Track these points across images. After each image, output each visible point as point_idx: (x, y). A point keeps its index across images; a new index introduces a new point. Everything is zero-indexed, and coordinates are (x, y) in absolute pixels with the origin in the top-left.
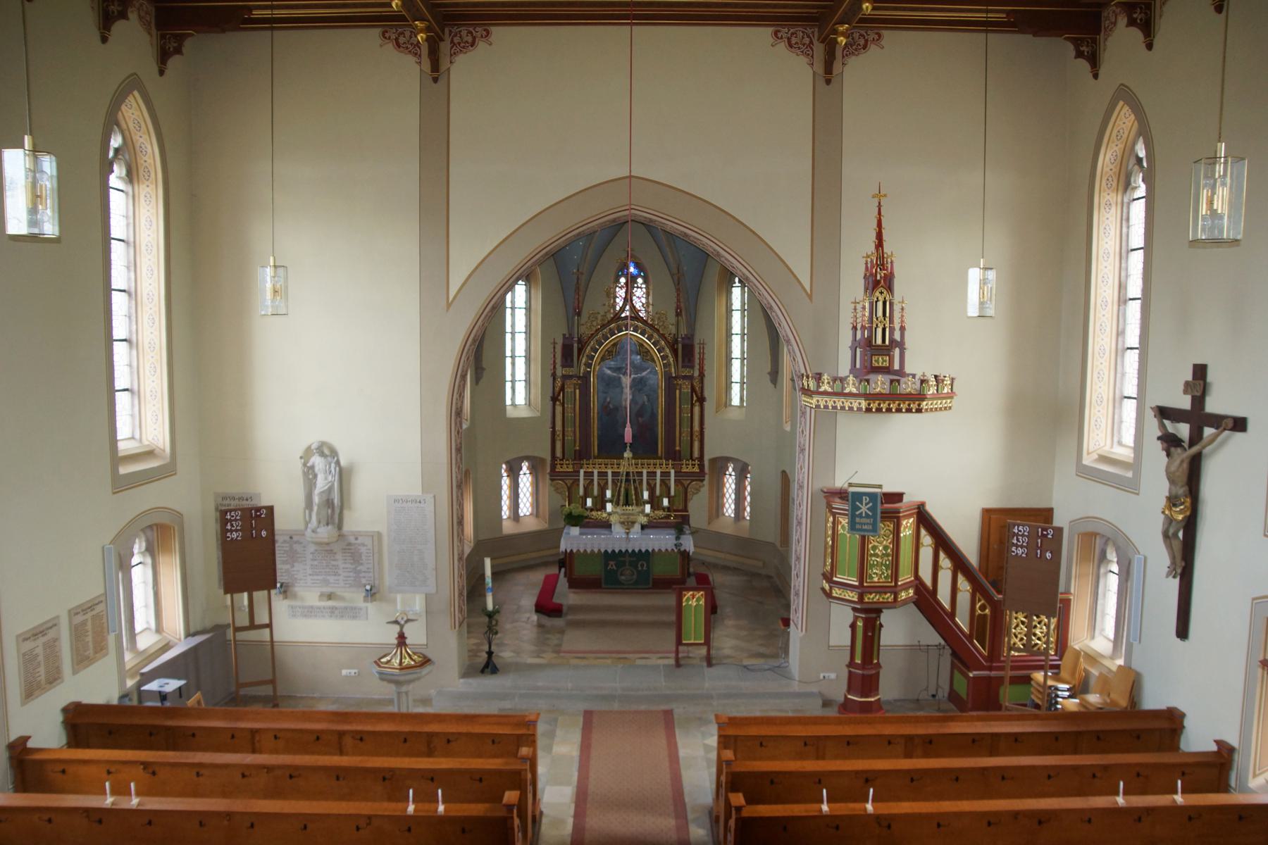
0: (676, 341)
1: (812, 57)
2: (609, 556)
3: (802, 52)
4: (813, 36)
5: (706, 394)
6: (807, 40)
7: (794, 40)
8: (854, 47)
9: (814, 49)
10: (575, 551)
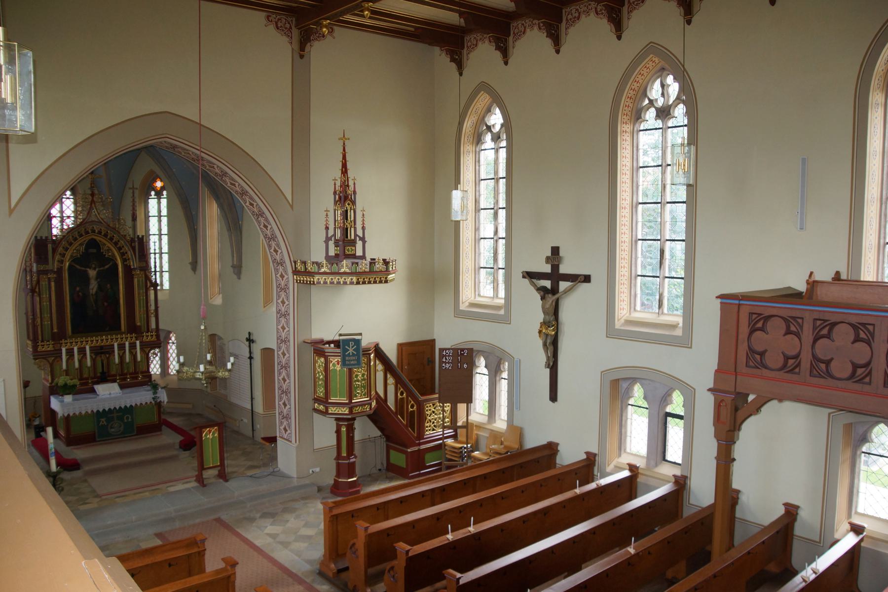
2: (100, 415)
10: (71, 415)
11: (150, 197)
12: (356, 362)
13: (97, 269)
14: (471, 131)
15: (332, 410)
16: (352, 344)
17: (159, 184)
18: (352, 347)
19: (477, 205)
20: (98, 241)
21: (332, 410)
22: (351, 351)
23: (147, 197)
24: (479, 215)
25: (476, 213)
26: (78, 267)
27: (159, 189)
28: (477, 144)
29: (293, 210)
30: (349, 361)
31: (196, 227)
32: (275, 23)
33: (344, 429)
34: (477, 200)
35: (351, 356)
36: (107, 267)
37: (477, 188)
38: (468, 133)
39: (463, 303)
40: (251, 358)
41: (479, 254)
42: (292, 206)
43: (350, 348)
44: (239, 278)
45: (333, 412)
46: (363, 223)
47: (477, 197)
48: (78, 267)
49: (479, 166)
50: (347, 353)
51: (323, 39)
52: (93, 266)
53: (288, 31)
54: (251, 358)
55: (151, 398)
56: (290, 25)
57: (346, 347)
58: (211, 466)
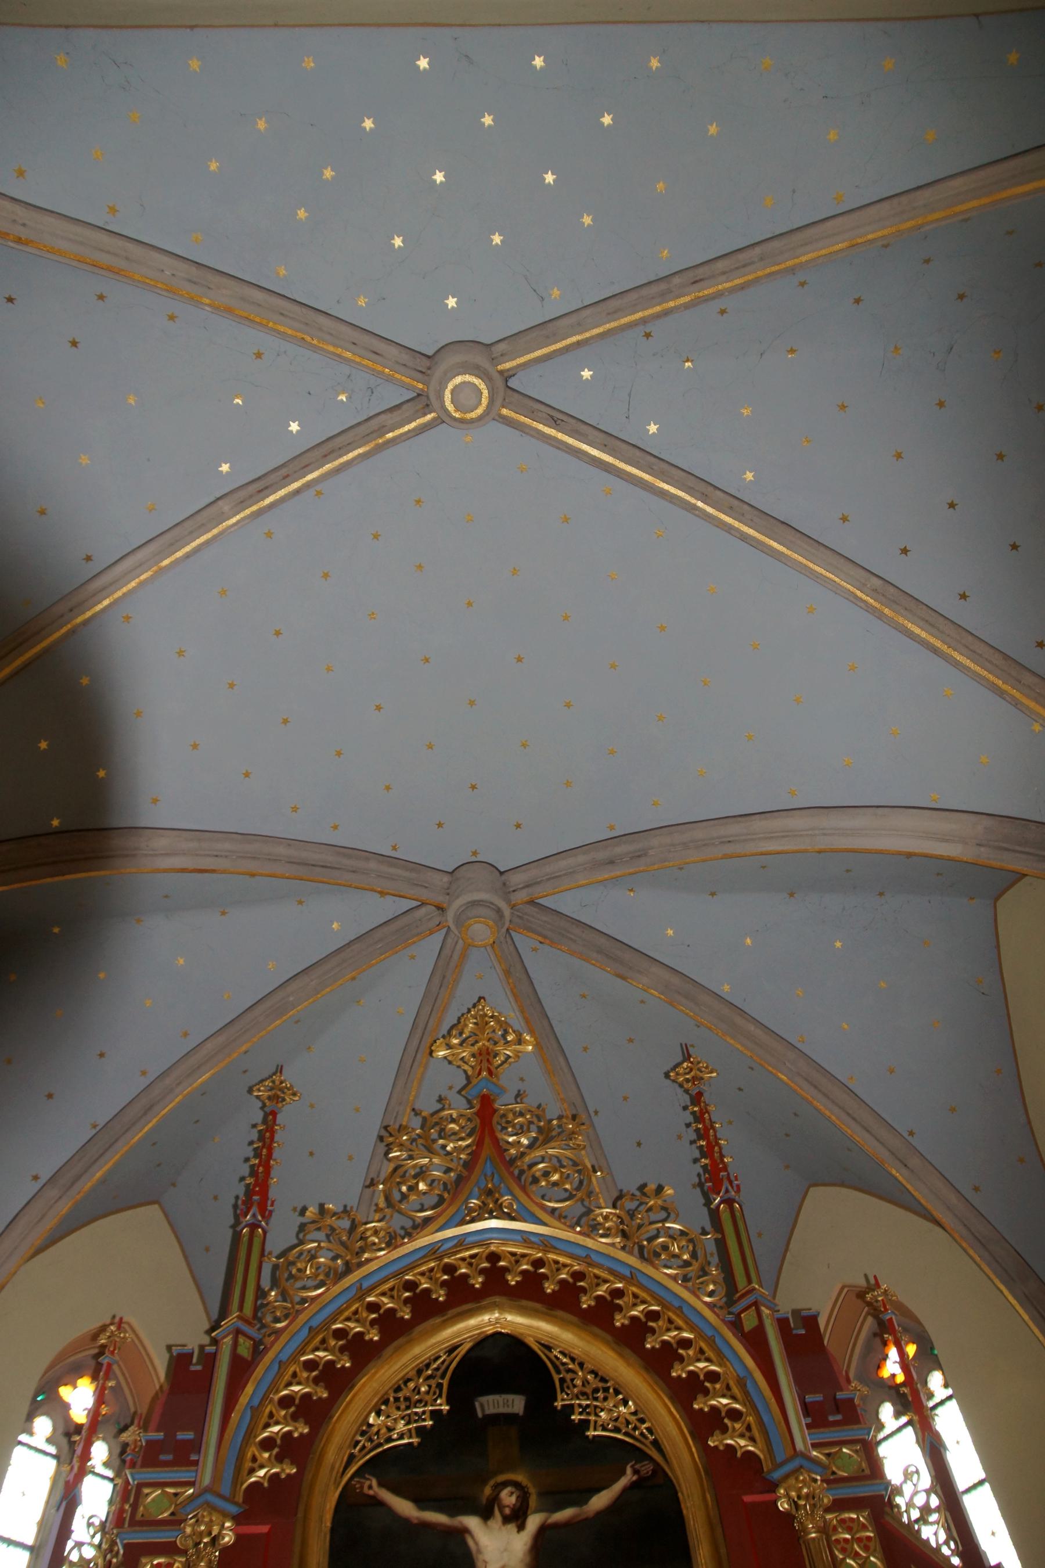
13: (534, 1522)
20: (535, 1347)
26: (404, 1507)
36: (600, 1501)
48: (404, 1507)
52: (509, 1498)
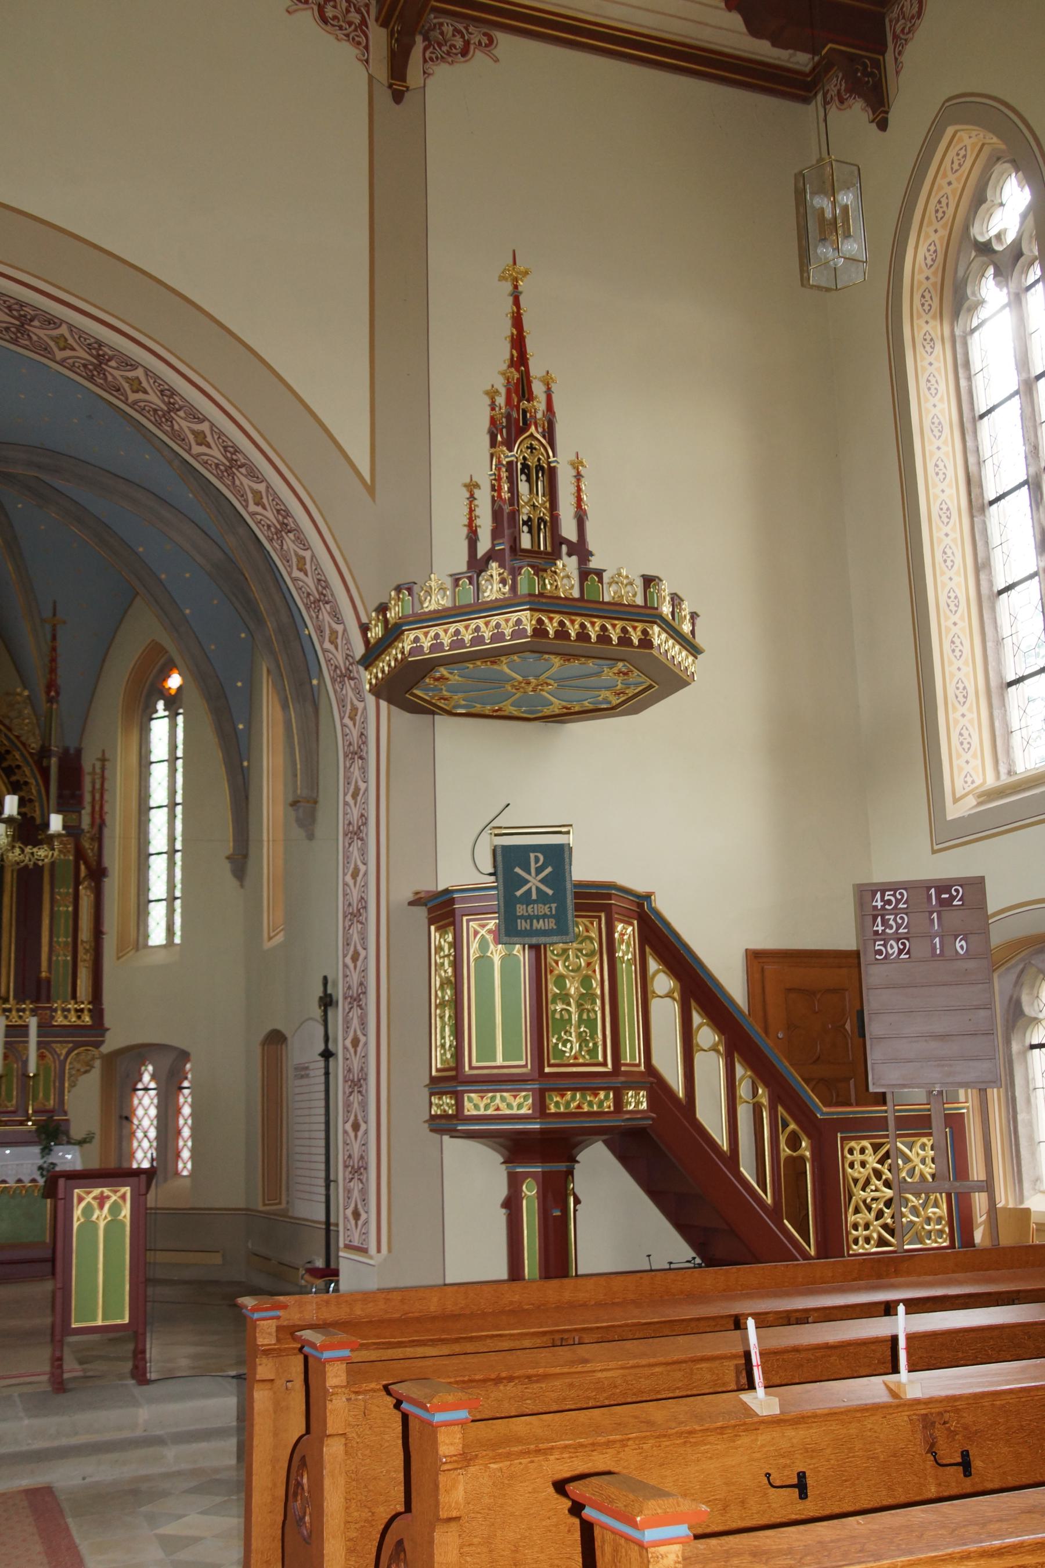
0: (44, 752)
1: (367, 48)
3: (347, 35)
4: (368, 13)
5: (107, 862)
6: (355, 18)
7: (330, 12)
8: (445, 49)
9: (370, 36)
11: (155, 716)
12: (551, 924)
14: (932, 279)
15: (477, 1107)
16: (537, 859)
17: (174, 681)
18: (539, 871)
19: (975, 491)
21: (475, 1104)
22: (534, 882)
23: (149, 714)
24: (984, 523)
25: (972, 517)
27: (173, 692)
28: (956, 315)
29: (374, 501)
30: (530, 918)
31: (245, 764)
32: (316, 8)
33: (530, 1191)
34: (974, 479)
35: (535, 902)
37: (970, 444)
38: (920, 283)
39: (956, 800)
40: (327, 1055)
41: (999, 642)
42: (371, 490)
43: (529, 873)
44: (311, 837)
45: (482, 1112)
46: (579, 500)
47: (973, 468)
49: (969, 378)
50: (518, 893)
51: (463, 59)
53: (355, 30)
54: (327, 1055)
55: (35, 1168)
56: (363, 17)
57: (518, 870)
58: (99, 1322)
